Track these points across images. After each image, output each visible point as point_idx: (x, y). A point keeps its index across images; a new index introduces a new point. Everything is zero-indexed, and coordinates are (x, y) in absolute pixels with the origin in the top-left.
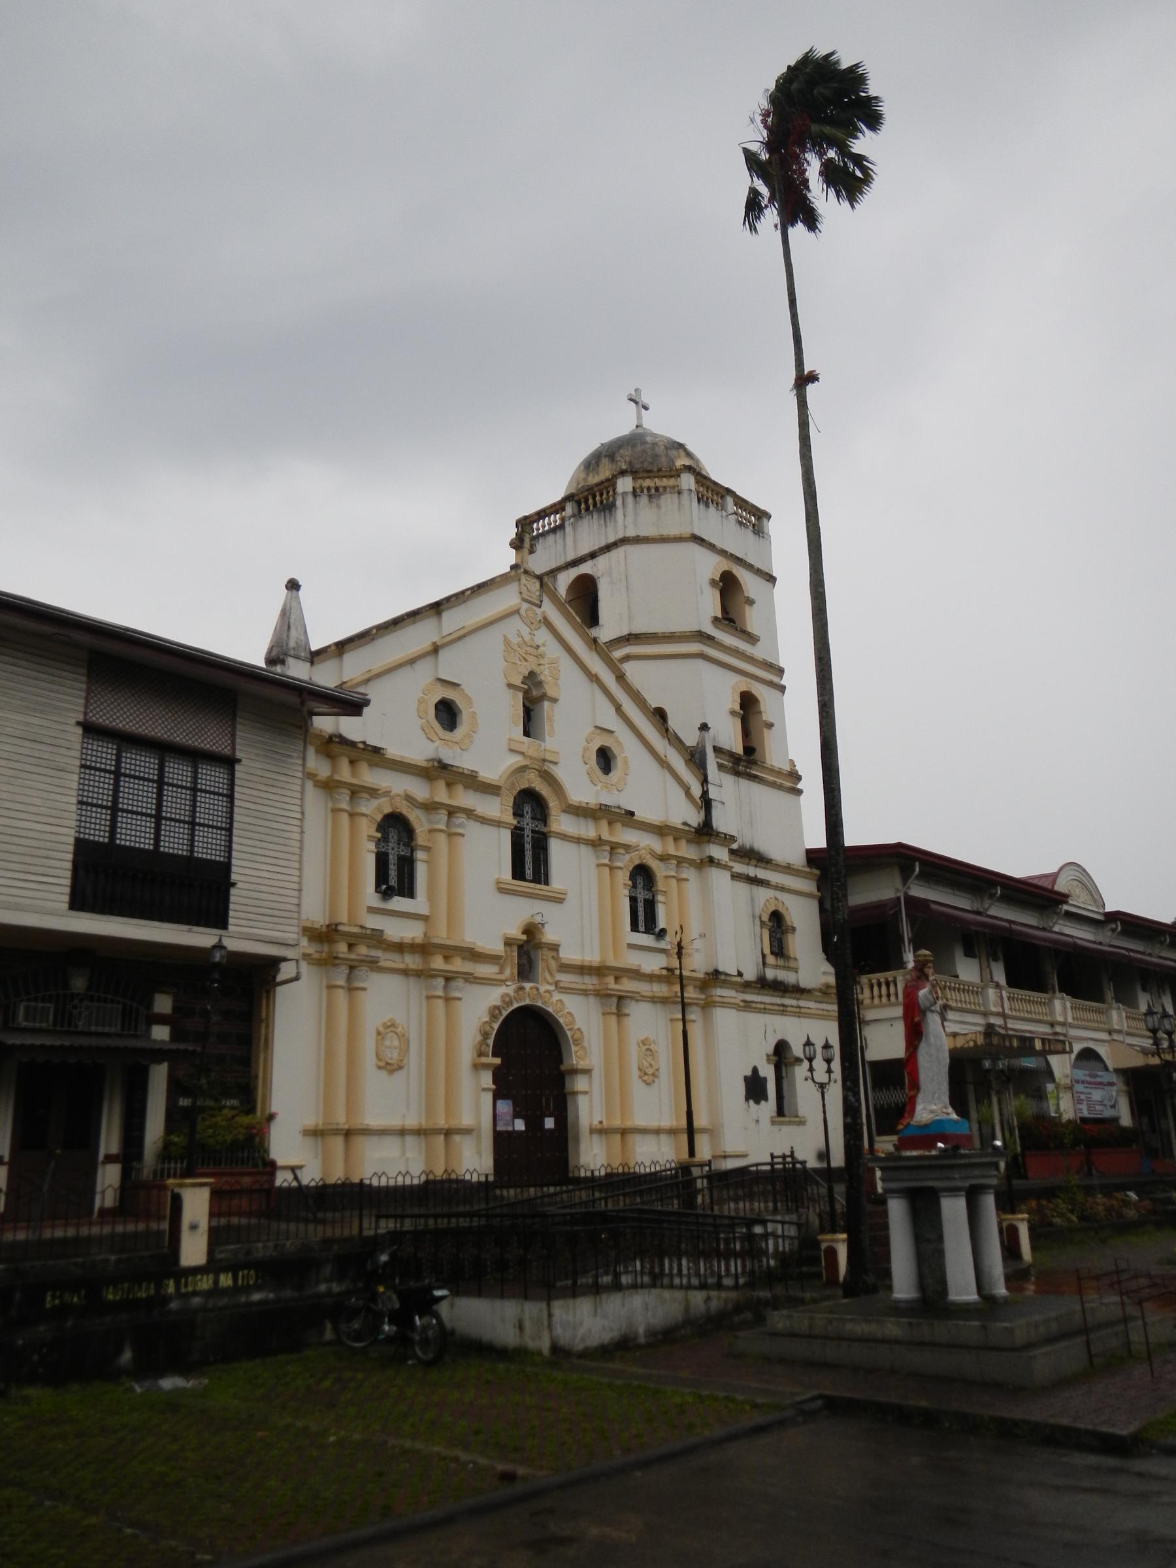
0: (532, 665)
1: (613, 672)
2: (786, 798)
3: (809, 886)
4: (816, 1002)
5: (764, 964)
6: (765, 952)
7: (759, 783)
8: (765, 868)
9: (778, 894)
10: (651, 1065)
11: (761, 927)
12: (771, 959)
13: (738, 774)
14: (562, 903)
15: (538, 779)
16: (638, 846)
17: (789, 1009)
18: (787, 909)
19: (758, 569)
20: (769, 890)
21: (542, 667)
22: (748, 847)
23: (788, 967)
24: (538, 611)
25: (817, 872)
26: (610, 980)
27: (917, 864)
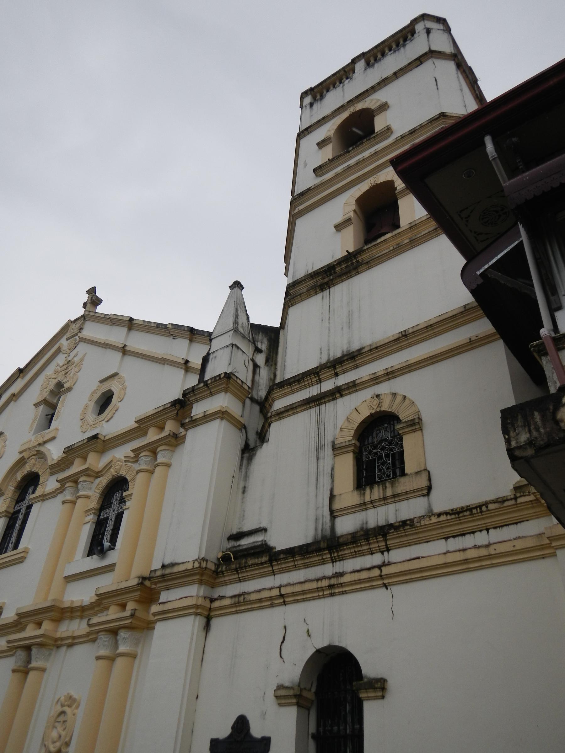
0: (60, 378)
1: (121, 326)
4: (446, 538)
5: (332, 512)
6: (336, 492)
7: (369, 268)
8: (357, 367)
9: (384, 388)
10: (60, 736)
11: (335, 455)
14: (22, 562)
15: (38, 460)
16: (112, 461)
17: (346, 579)
18: (405, 397)
19: (395, 74)
20: (359, 393)
21: (67, 375)
23: (397, 495)
24: (77, 337)
26: (47, 626)
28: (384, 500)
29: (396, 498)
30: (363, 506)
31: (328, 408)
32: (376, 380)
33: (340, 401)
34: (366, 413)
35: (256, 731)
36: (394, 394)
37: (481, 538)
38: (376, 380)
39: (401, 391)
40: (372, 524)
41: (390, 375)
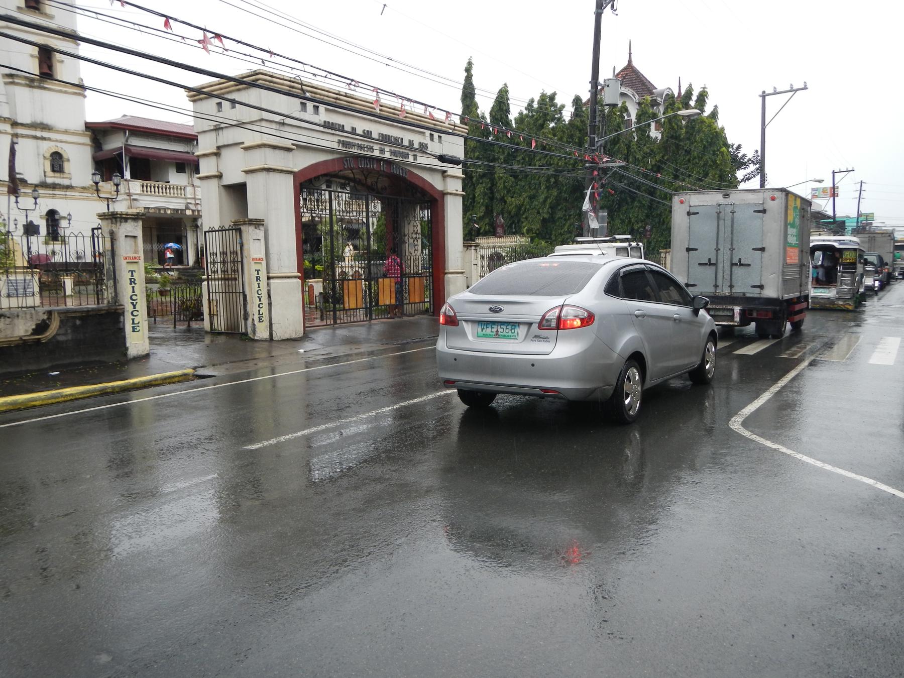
2: (82, 98)
3: (87, 140)
5: (45, 176)
9: (58, 144)
12: (50, 173)
13: (31, 87)
22: (39, 122)
25: (90, 133)
27: (127, 132)
28: (60, 177)
29: (63, 178)
30: (55, 177)
31: (40, 142)
32: (57, 141)
33: (45, 142)
34: (54, 151)
35: (36, 223)
36: (62, 148)
37: (86, 194)
38: (57, 141)
39: (64, 148)
40: (57, 182)
41: (61, 142)
